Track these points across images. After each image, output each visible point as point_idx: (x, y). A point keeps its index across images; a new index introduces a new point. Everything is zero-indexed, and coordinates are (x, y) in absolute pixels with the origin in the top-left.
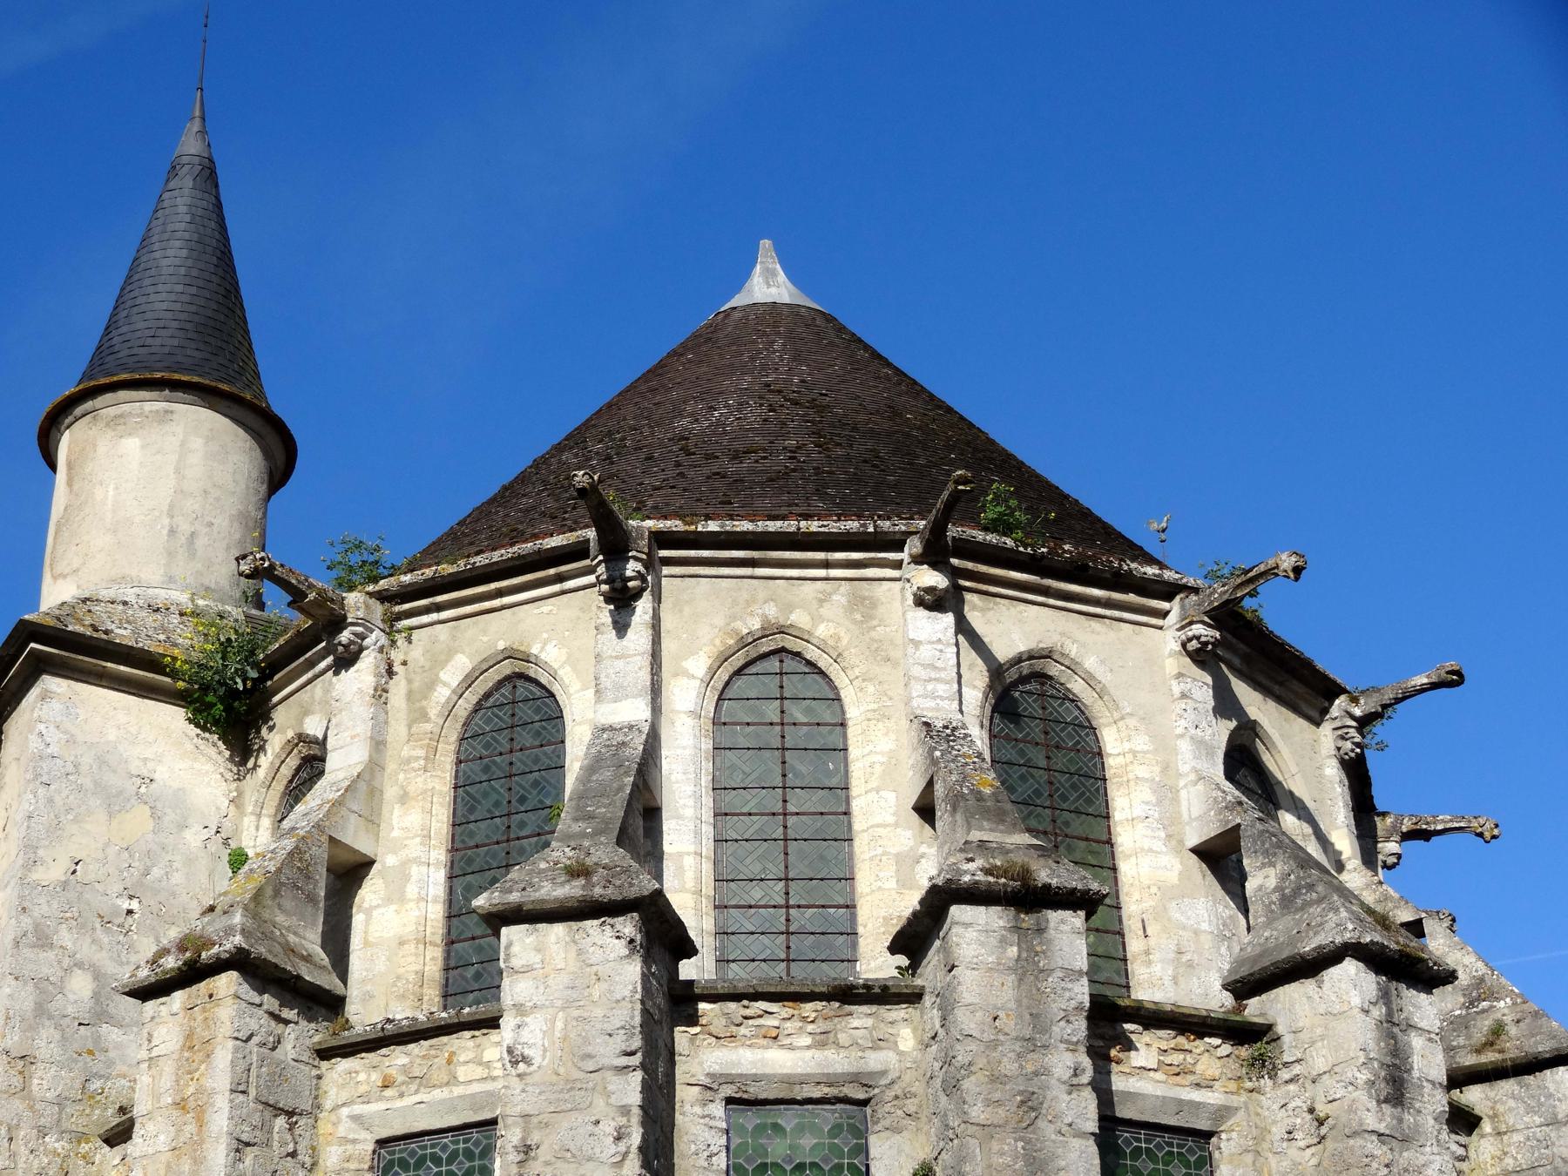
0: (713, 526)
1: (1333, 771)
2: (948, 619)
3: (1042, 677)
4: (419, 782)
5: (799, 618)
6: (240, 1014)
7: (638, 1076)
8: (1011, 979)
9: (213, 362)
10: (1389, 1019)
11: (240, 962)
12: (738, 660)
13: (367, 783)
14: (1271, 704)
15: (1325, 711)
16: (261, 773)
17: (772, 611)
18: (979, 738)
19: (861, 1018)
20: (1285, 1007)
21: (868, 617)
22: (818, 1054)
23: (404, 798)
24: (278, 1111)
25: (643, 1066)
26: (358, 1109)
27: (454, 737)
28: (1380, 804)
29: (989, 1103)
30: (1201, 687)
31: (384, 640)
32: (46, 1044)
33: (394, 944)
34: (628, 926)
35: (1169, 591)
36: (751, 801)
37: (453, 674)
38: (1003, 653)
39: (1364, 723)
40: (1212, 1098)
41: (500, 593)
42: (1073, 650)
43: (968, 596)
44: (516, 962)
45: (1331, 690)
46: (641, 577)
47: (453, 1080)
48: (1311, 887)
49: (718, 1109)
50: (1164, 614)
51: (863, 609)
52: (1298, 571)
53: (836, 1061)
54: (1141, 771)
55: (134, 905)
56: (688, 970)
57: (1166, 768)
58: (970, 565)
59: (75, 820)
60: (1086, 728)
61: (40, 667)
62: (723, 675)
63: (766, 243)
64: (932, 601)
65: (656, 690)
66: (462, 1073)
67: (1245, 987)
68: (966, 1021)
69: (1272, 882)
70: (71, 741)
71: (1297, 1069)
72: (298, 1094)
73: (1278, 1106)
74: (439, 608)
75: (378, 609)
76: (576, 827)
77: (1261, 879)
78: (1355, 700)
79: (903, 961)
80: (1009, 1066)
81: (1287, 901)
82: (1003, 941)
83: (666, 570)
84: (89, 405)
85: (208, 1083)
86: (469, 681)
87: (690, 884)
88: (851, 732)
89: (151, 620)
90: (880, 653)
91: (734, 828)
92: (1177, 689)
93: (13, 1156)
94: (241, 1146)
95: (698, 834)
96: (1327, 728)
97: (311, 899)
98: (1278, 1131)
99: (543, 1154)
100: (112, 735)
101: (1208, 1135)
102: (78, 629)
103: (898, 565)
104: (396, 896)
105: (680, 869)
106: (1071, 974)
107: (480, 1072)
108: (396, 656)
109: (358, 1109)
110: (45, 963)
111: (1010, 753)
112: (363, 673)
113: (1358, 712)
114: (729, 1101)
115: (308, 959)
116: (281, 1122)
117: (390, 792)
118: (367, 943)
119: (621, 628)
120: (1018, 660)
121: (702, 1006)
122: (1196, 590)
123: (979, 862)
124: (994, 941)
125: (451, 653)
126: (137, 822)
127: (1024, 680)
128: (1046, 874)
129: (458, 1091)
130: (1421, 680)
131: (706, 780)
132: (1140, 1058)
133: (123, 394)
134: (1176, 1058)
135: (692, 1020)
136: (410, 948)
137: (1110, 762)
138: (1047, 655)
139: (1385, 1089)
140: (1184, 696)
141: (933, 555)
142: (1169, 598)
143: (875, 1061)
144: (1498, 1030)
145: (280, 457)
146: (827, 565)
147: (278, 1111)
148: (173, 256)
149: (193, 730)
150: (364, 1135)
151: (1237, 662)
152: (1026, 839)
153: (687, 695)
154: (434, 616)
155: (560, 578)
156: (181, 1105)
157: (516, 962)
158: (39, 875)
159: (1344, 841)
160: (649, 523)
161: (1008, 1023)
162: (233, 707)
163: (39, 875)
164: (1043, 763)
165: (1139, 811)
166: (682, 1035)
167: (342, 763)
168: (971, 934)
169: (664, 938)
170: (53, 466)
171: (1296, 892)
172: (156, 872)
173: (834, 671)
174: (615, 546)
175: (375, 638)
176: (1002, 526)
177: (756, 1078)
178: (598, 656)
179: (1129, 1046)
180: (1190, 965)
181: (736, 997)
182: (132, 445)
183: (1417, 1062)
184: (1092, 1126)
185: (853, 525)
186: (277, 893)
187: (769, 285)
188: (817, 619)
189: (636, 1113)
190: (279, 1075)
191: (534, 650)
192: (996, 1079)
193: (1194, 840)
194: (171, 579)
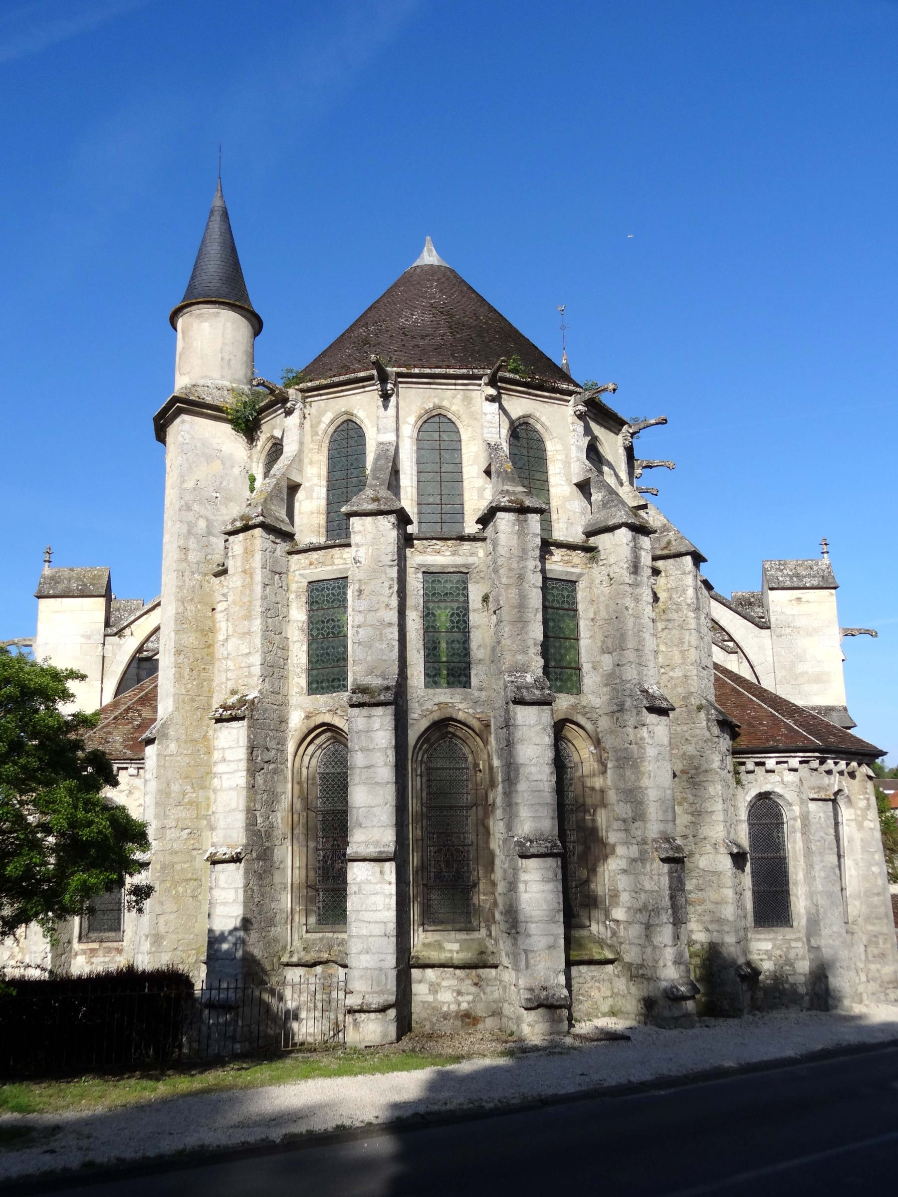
0: (417, 371)
1: (622, 452)
2: (497, 405)
3: (527, 424)
4: (316, 457)
5: (445, 403)
6: (263, 542)
7: (396, 568)
8: (516, 537)
9: (233, 294)
10: (635, 547)
11: (262, 525)
12: (425, 417)
13: (298, 458)
14: (603, 429)
15: (620, 430)
16: (259, 448)
17: (436, 401)
18: (505, 446)
19: (466, 546)
20: (602, 541)
21: (469, 403)
22: (452, 558)
23: (311, 463)
24: (276, 573)
25: (398, 565)
26: (302, 572)
27: (327, 441)
28: (636, 457)
29: (508, 577)
30: (580, 427)
31: (302, 406)
32: (192, 544)
33: (310, 512)
34: (392, 518)
35: (570, 393)
36: (429, 467)
37: (327, 418)
38: (514, 416)
39: (632, 435)
40: (577, 570)
41: (342, 391)
42: (537, 414)
43: (503, 396)
44: (355, 530)
45: (622, 423)
46: (392, 389)
47: (333, 564)
48: (612, 501)
49: (420, 575)
50: (569, 401)
51: (468, 400)
52: (614, 390)
53: (459, 560)
54: (559, 457)
55: (218, 495)
56: (410, 529)
57: (566, 457)
58: (504, 385)
59: (196, 466)
60: (541, 441)
61: (180, 412)
62: (420, 423)
63: (428, 238)
64: (491, 399)
65: (398, 429)
66: (336, 561)
67: (590, 533)
68: (502, 550)
69: (600, 498)
70: (193, 438)
71: (605, 562)
72: (282, 567)
73: (598, 573)
74: (321, 395)
75: (300, 395)
76: (374, 482)
77: (597, 496)
78: (630, 427)
79: (481, 527)
80: (515, 565)
81: (605, 505)
82: (513, 524)
83: (400, 385)
84: (189, 309)
85: (254, 565)
86: (332, 422)
87: (409, 497)
88: (463, 444)
89: (217, 393)
90: (473, 416)
91: (425, 477)
92: (572, 428)
93: (184, 581)
95: (412, 479)
96: (620, 436)
97: (282, 500)
98: (598, 581)
99: (366, 592)
100: (207, 435)
101: (576, 582)
102: (193, 398)
103: (480, 385)
104: (310, 497)
105: (406, 492)
106: (536, 535)
107: (342, 561)
108: (306, 411)
109: (302, 572)
110: (190, 516)
111: (516, 451)
112: (295, 417)
113: (631, 431)
114: (424, 572)
115: (282, 521)
116: (277, 576)
117: (306, 461)
118: (300, 513)
119: (386, 407)
120: (519, 418)
121: (415, 542)
122: (580, 393)
123: (507, 498)
124: (511, 524)
125: (326, 411)
126: (217, 466)
127: (521, 425)
128: (528, 503)
129: (335, 567)
130: (653, 421)
131: (414, 460)
132: (554, 558)
133: (201, 306)
134: (566, 558)
135: (412, 546)
136: (315, 515)
137: (548, 453)
138: (529, 416)
139: (632, 570)
140: (574, 430)
141: (492, 383)
142: (570, 395)
143: (471, 560)
144: (669, 543)
145: (257, 327)
146: (455, 384)
147: (276, 573)
148: (214, 249)
149: (234, 432)
150: (304, 580)
151: (592, 416)
152: (521, 489)
153: (408, 430)
154: (319, 398)
155: (364, 387)
156: (244, 571)
157: (355, 530)
158: (185, 486)
159: (624, 476)
160: (395, 369)
161: (514, 551)
162: (248, 427)
163: (185, 486)
164: (526, 454)
165: (558, 471)
166: (409, 551)
167: (290, 448)
168: (503, 522)
169: (403, 519)
170: (176, 330)
171: (608, 502)
172: (225, 483)
173: (457, 422)
174: (383, 378)
175: (299, 405)
176: (515, 371)
177: (433, 566)
178: (378, 417)
179: (552, 554)
180: (572, 523)
181: (426, 539)
182: (206, 325)
183: (642, 560)
184: (540, 585)
185: (465, 371)
186: (271, 499)
187: (429, 257)
188: (452, 404)
189: (396, 580)
190: (276, 561)
191: (355, 412)
192: (510, 570)
193: (575, 481)
194: (223, 377)
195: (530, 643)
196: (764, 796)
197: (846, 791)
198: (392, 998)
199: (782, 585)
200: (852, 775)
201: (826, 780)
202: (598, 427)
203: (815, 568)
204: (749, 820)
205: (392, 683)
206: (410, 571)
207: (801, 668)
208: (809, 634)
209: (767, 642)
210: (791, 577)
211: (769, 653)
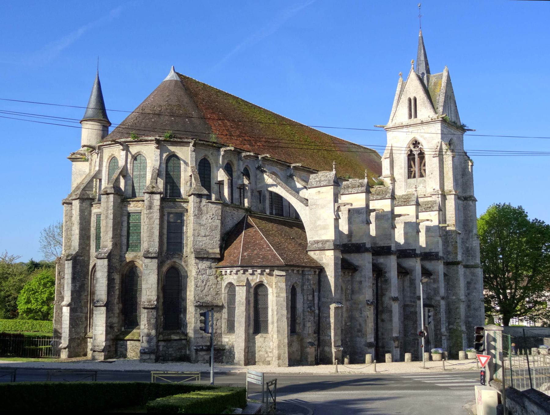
5: (114, 153)
14: (178, 147)
38: (133, 153)
42: (142, 151)
94: (66, 222)
128: (109, 192)
132: (132, 205)
153: (105, 164)
179: (130, 204)
195: (108, 238)
196: (231, 284)
197: (265, 281)
198: (66, 345)
199: (312, 186)
200: (270, 274)
201: (250, 278)
202: (175, 147)
203: (328, 176)
204: (228, 292)
205: (74, 253)
206: (92, 215)
207: (318, 223)
208: (322, 208)
209: (308, 212)
210: (317, 181)
211: (308, 217)
